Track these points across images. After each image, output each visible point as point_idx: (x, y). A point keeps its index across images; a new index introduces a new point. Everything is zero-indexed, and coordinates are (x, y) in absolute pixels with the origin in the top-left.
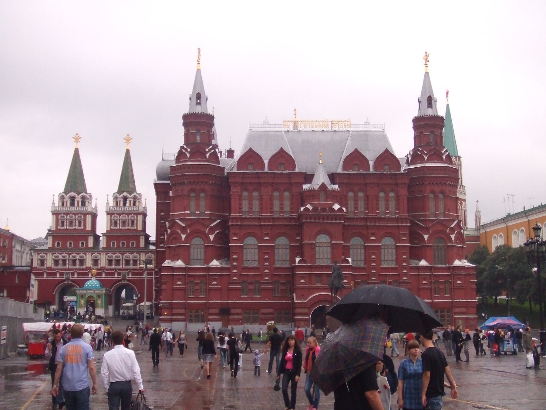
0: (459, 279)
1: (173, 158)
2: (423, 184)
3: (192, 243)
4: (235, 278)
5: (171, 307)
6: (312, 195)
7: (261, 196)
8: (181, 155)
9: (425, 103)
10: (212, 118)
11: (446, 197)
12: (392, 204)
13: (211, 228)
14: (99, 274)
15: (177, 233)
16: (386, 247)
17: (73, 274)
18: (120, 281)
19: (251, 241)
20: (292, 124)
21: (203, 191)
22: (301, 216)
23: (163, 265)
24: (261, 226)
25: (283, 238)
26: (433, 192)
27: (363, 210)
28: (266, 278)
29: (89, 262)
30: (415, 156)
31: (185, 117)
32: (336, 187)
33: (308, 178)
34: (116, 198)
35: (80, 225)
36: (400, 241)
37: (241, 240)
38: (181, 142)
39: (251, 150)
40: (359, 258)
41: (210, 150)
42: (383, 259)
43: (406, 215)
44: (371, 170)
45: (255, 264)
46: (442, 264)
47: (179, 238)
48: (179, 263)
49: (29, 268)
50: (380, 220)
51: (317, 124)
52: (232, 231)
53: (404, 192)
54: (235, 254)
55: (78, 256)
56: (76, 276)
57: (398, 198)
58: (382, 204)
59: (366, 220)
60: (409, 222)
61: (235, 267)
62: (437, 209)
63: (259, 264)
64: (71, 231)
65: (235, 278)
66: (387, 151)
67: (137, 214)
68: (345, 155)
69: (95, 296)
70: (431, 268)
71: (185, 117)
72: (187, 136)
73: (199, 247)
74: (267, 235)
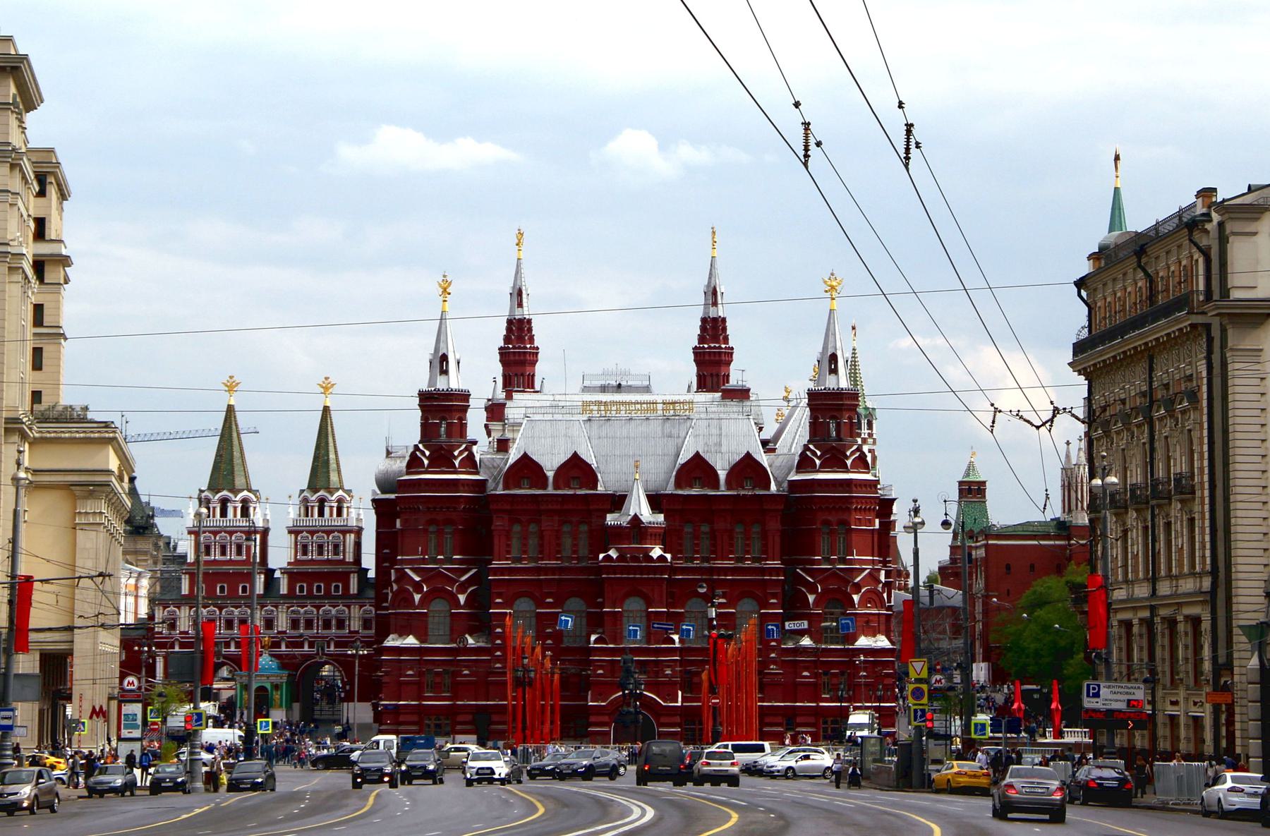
7: (541, 532)
8: (414, 462)
17: (227, 645)
22: (599, 570)
30: (805, 463)
32: (661, 518)
34: (305, 500)
43: (776, 564)
46: (837, 643)
48: (411, 641)
53: (774, 525)
55: (236, 612)
57: (764, 535)
61: (499, 648)
67: (344, 532)
69: (268, 686)
72: (426, 427)
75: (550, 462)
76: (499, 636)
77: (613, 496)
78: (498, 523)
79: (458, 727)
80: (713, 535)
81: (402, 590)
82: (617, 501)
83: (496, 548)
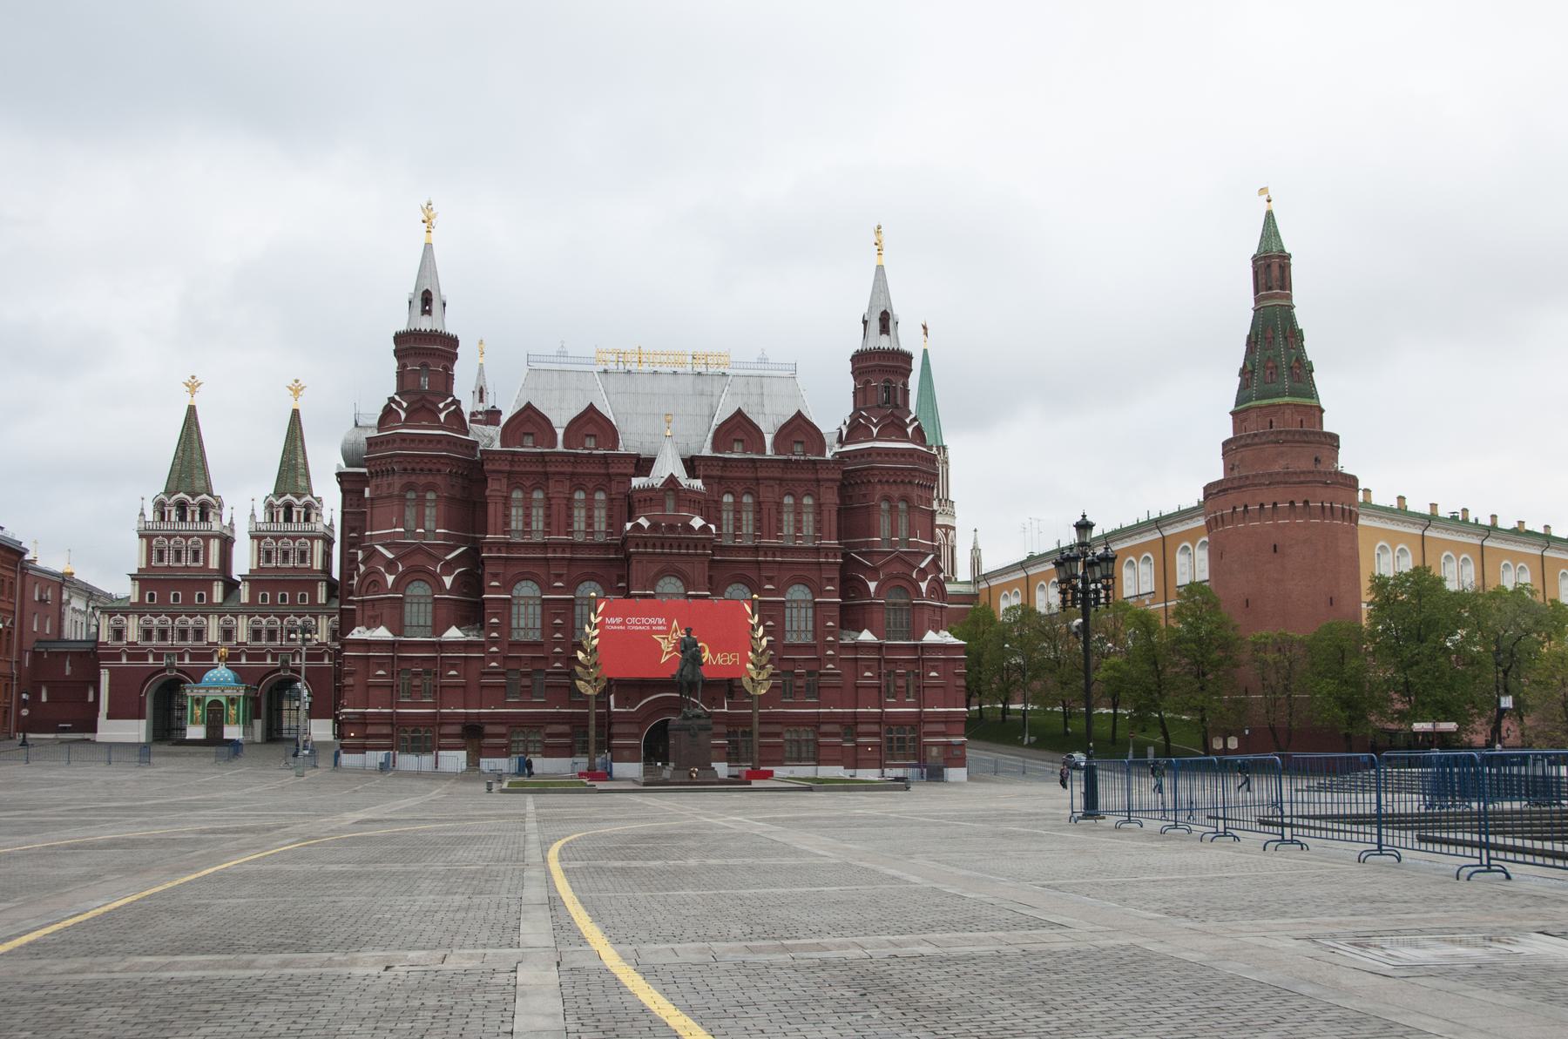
0: (934, 668)
1: (375, 422)
3: (408, 592)
5: (364, 720)
6: (651, 497)
8: (388, 414)
9: (875, 325)
10: (453, 342)
11: (911, 508)
12: (808, 520)
13: (448, 563)
14: (234, 656)
15: (378, 572)
17: (181, 658)
18: (278, 670)
19: (527, 589)
20: (614, 358)
21: (430, 487)
22: (626, 540)
23: (350, 636)
24: (546, 559)
26: (888, 499)
27: (751, 530)
29: (213, 634)
30: (856, 429)
31: (399, 338)
32: (698, 484)
33: (644, 465)
34: (270, 506)
35: (196, 559)
36: (822, 593)
37: (508, 586)
38: (390, 388)
39: (529, 406)
41: (447, 406)
42: (788, 627)
44: (769, 451)
45: (535, 636)
47: (378, 583)
48: (382, 633)
49: (91, 645)
50: (784, 550)
51: (664, 358)
52: (489, 570)
53: (831, 498)
54: (495, 615)
55: (191, 622)
56: (187, 661)
57: (819, 508)
58: (788, 518)
59: (756, 549)
61: (494, 642)
62: (894, 532)
63: (543, 635)
64: (178, 569)
66: (799, 414)
67: (312, 539)
68: (717, 421)
70: (880, 646)
71: (399, 338)
74: (559, 577)
75: (560, 417)
76: (494, 627)
77: (637, 457)
78: (494, 487)
79: (443, 741)
80: (758, 505)
81: (371, 572)
82: (644, 465)
83: (491, 520)
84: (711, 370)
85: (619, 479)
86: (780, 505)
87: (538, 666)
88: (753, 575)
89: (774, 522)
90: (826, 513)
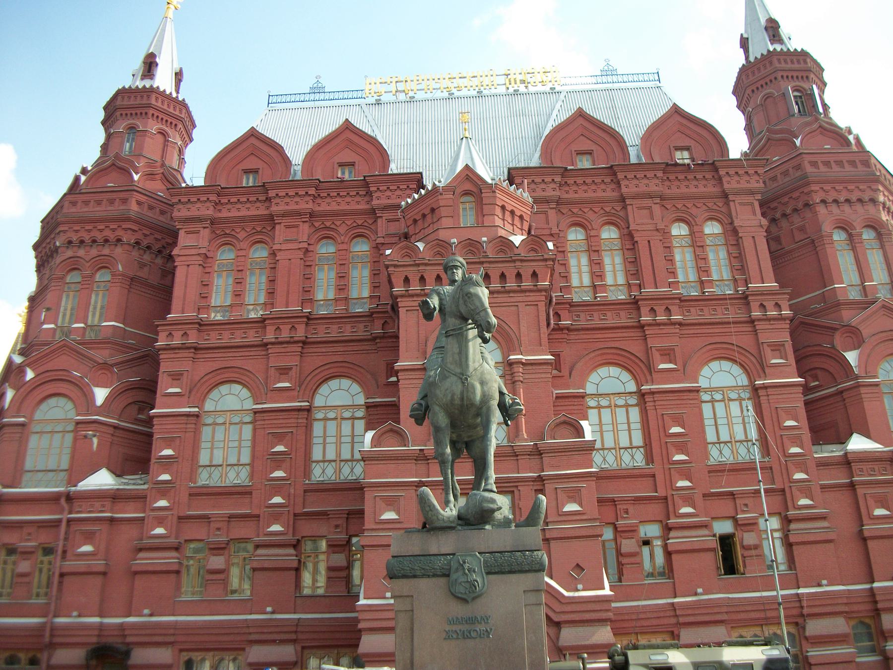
2: (807, 205)
4: (160, 531)
16: (718, 396)
21: (103, 264)
25: (346, 383)
27: (621, 280)
28: (276, 528)
40: (624, 442)
42: (711, 436)
45: (238, 477)
52: (165, 367)
58: (683, 258)
60: (785, 304)
61: (163, 489)
63: (252, 476)
65: (160, 531)
73: (59, 428)
74: (284, 372)
76: (167, 463)
84: (532, 89)
85: (387, 215)
86: (665, 234)
87: (240, 530)
88: (636, 348)
89: (660, 263)
90: (747, 244)
